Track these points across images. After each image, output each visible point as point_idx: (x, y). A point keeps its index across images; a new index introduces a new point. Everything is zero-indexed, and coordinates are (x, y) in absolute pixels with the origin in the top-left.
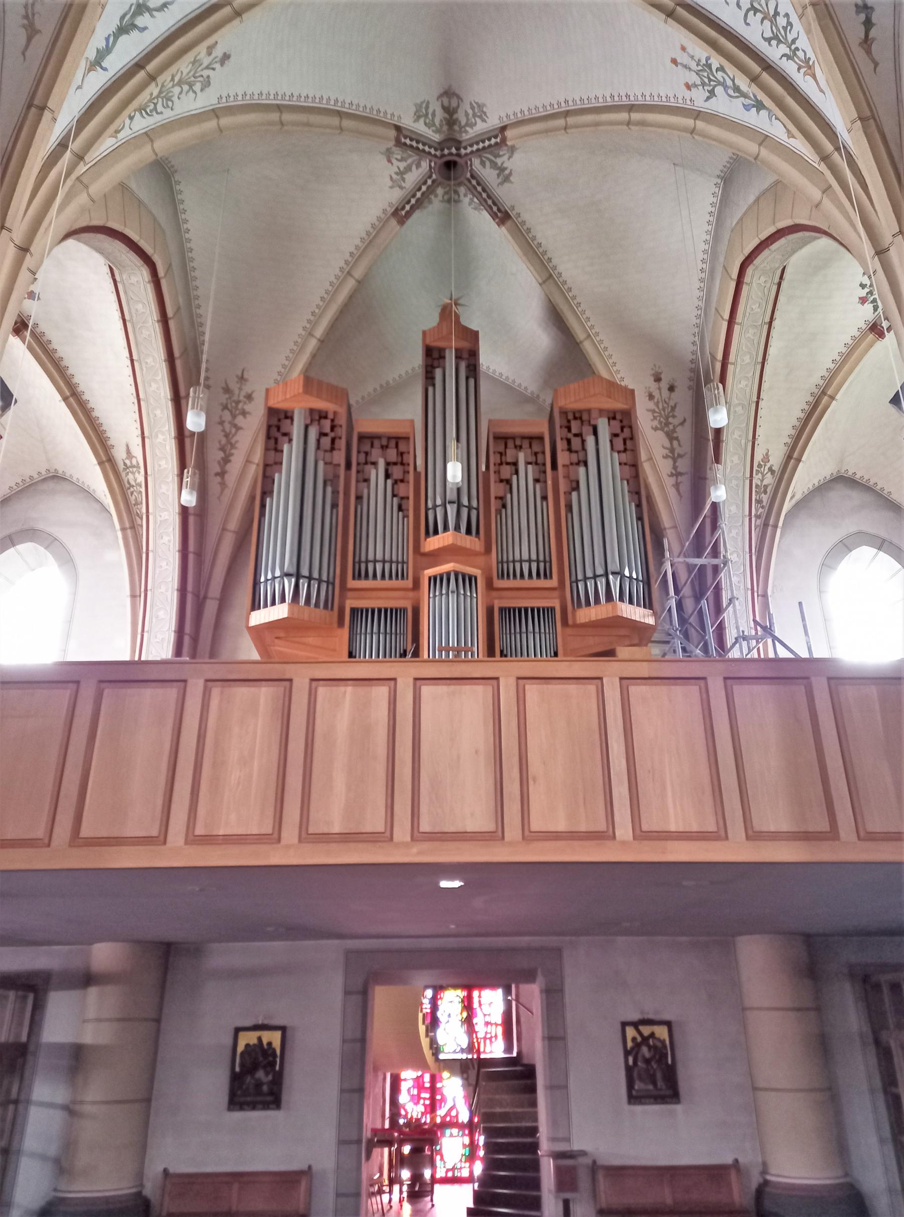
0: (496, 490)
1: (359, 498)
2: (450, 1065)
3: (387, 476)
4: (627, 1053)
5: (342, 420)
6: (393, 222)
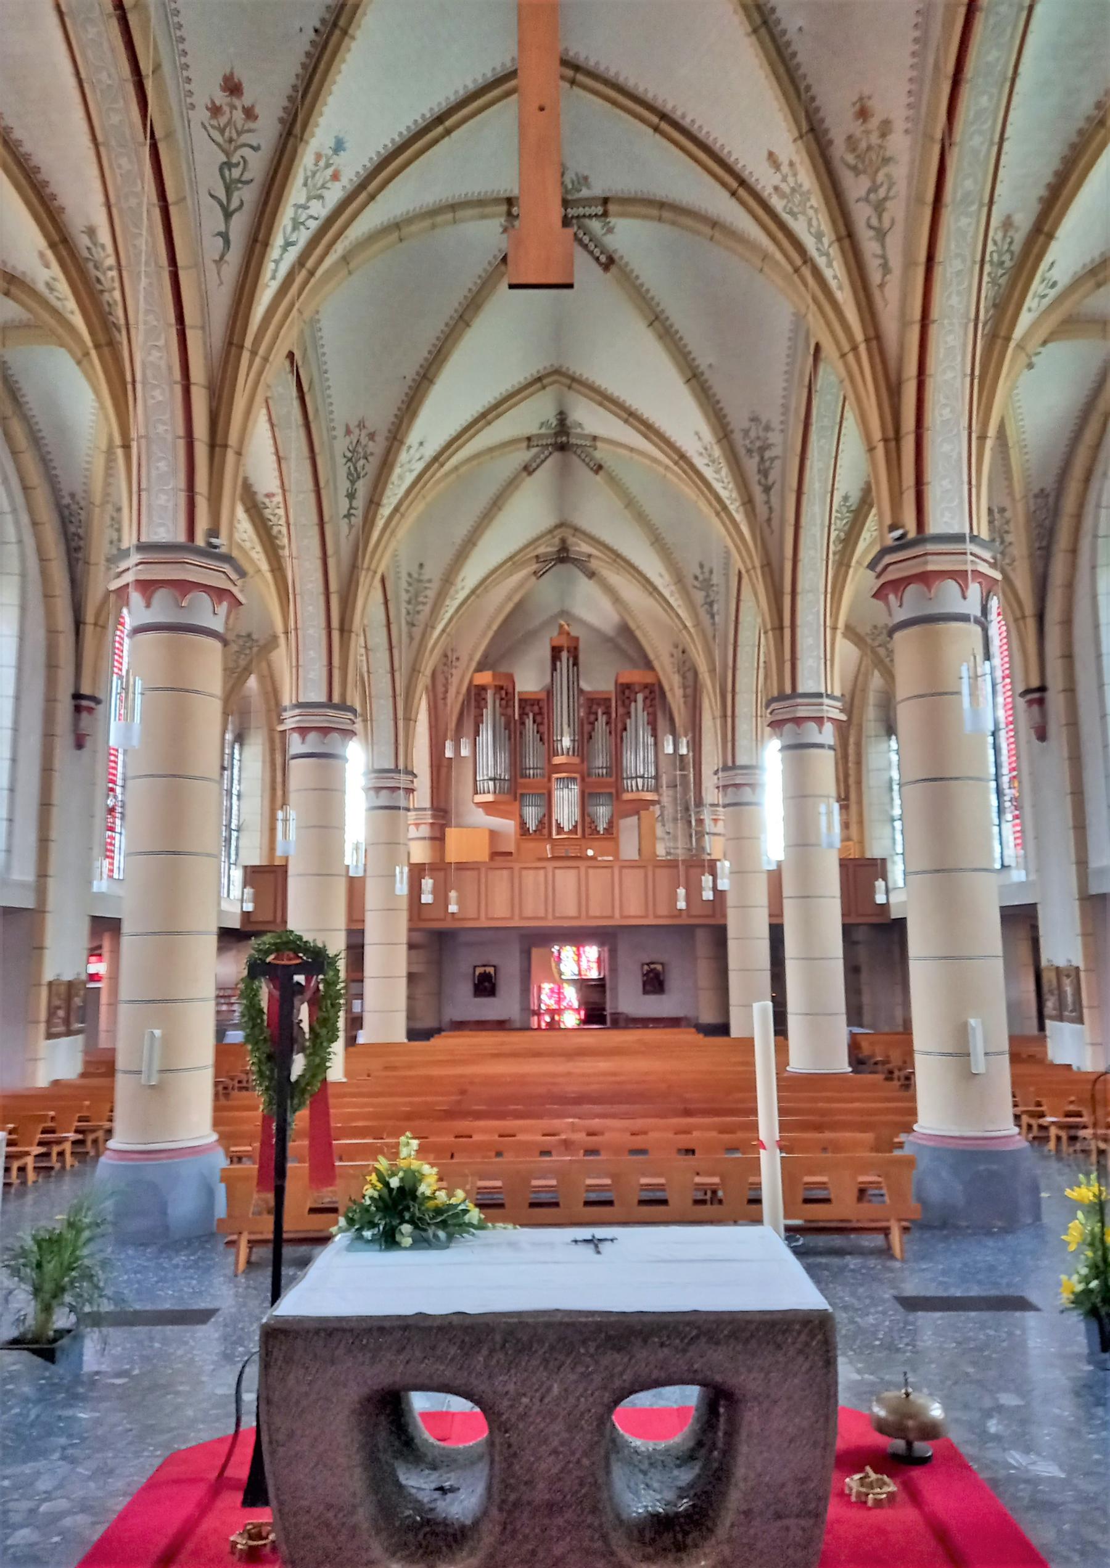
0: (587, 728)
1: (521, 733)
2: (568, 981)
3: (534, 722)
4: (644, 975)
5: (510, 690)
6: (534, 579)
